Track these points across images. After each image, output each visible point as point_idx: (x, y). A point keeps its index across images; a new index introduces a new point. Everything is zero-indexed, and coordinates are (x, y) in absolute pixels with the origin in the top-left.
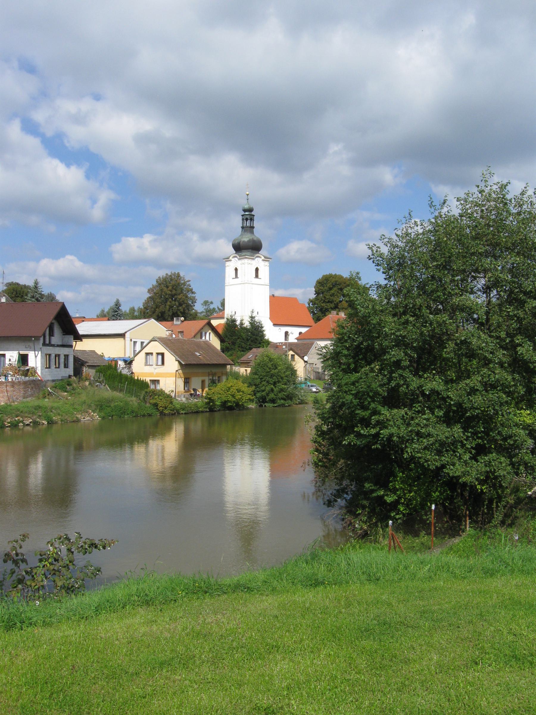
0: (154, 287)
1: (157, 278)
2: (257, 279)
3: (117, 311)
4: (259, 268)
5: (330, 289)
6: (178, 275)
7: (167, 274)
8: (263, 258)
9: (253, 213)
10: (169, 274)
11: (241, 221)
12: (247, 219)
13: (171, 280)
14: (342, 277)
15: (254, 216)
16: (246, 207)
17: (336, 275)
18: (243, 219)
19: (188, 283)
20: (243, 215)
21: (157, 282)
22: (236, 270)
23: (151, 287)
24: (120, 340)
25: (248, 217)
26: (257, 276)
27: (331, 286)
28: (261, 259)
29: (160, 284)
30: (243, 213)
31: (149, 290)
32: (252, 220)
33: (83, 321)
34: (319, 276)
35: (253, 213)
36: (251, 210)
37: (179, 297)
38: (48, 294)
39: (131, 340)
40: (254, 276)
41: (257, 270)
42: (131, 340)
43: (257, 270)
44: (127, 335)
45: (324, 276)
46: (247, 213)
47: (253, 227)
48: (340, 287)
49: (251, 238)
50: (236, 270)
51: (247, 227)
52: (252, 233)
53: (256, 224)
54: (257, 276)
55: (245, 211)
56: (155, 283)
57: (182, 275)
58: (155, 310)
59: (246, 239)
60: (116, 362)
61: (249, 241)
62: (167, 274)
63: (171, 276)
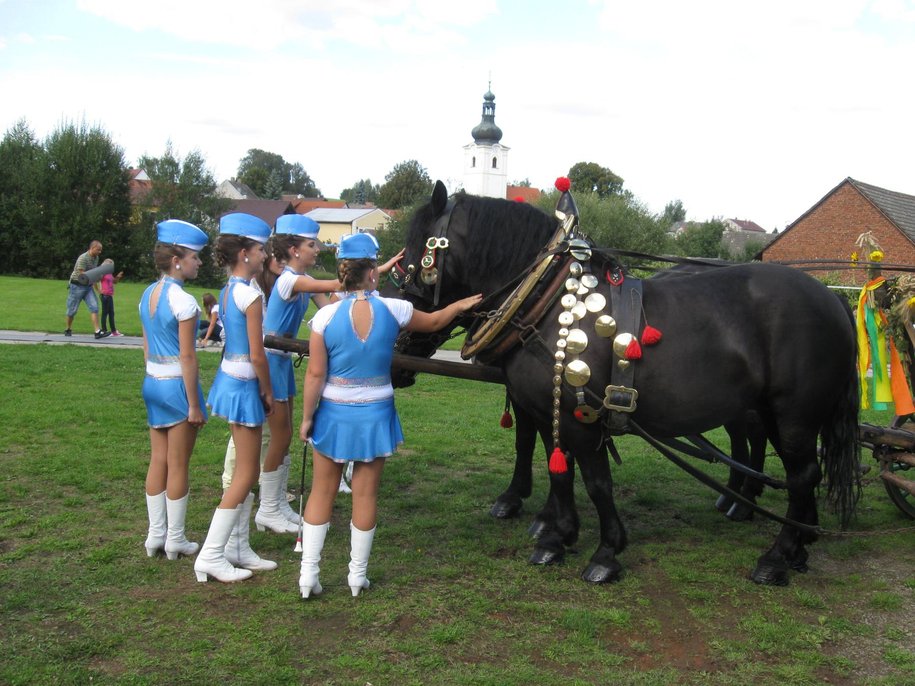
0: (391, 174)
1: (395, 165)
2: (494, 169)
3: (360, 193)
4: (497, 157)
5: (582, 178)
6: (416, 163)
7: (405, 161)
8: (501, 148)
9: (494, 101)
10: (407, 161)
13: (409, 166)
14: (596, 165)
16: (488, 95)
17: (590, 164)
18: (484, 108)
19: (425, 171)
20: (484, 104)
21: (395, 168)
22: (474, 159)
23: (389, 174)
24: (349, 226)
25: (489, 105)
26: (494, 165)
27: (583, 176)
28: (499, 150)
29: (397, 171)
30: (484, 101)
31: (386, 177)
32: (493, 108)
33: (318, 207)
34: (572, 165)
35: (494, 101)
37: (414, 185)
38: (295, 164)
39: (357, 228)
40: (492, 165)
41: (495, 160)
42: (357, 228)
43: (495, 160)
44: (354, 224)
45: (577, 164)
46: (488, 102)
48: (591, 177)
49: (490, 127)
50: (474, 159)
51: (487, 116)
54: (494, 165)
56: (392, 170)
57: (419, 162)
58: (391, 197)
59: (485, 128)
60: (335, 249)
61: (488, 130)
62: (405, 161)
63: (408, 163)
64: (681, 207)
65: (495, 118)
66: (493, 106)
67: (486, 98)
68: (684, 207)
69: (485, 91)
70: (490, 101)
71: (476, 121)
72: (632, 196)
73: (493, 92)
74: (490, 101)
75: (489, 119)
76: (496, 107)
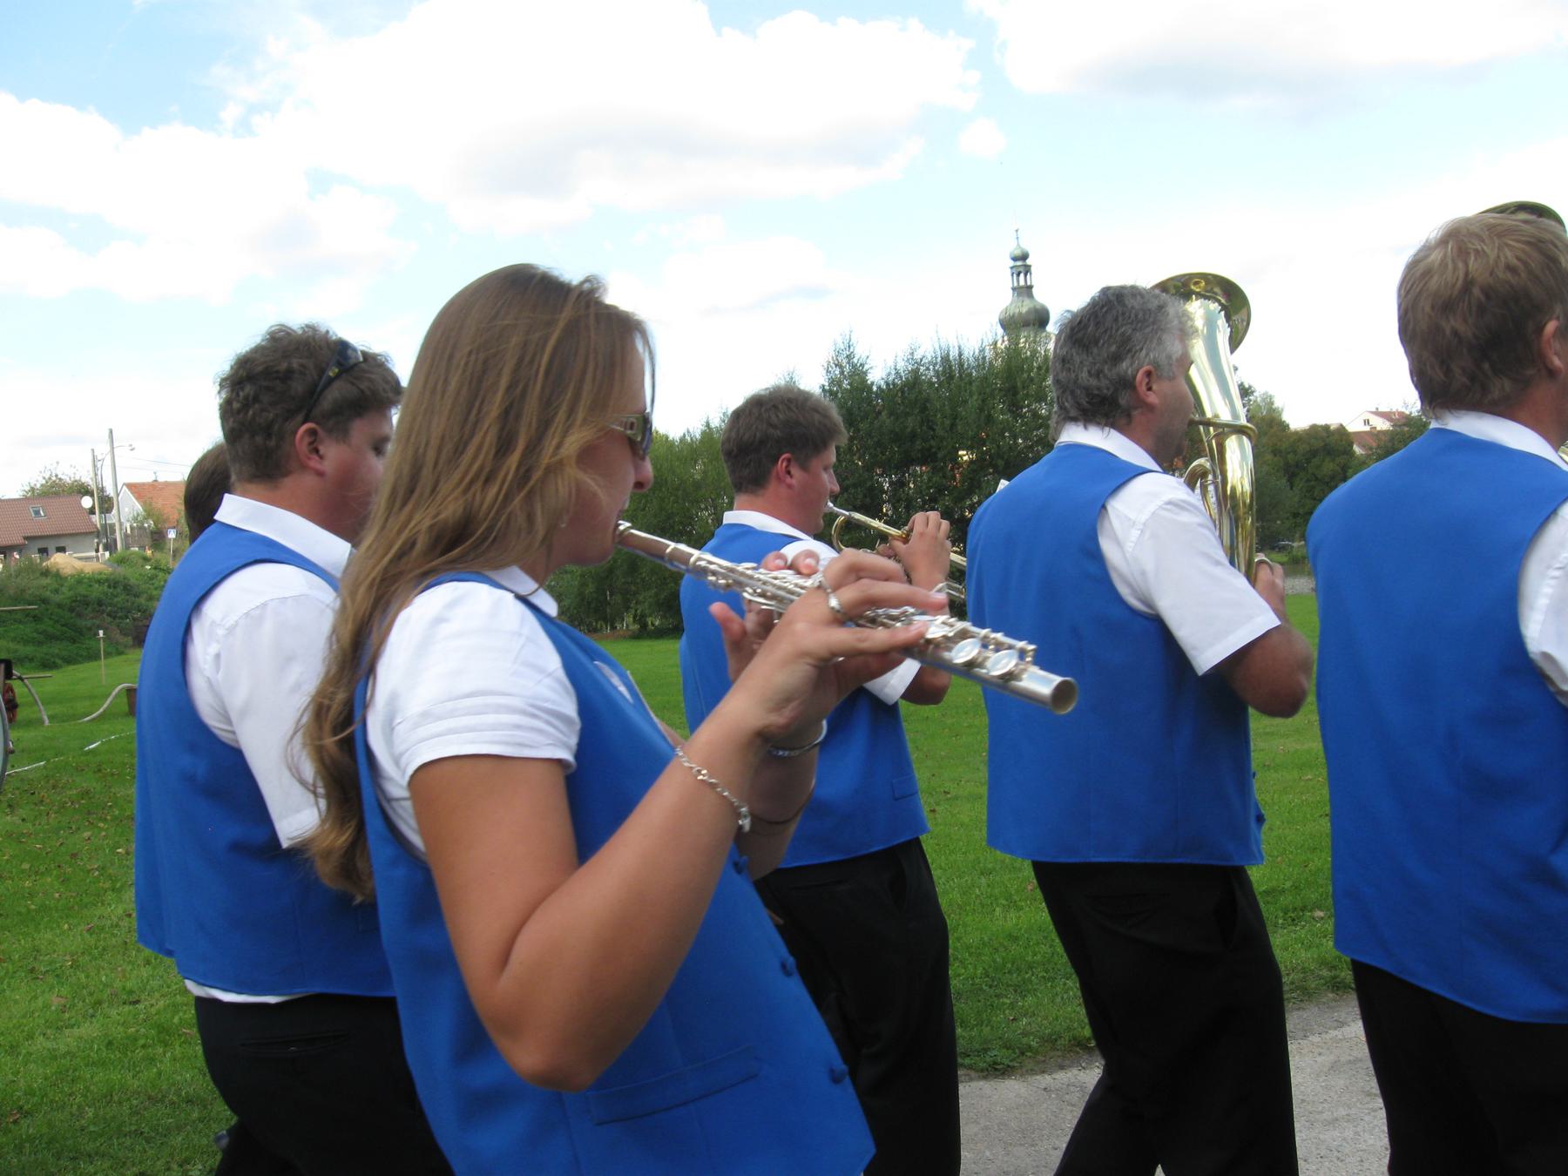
9: (1028, 262)
11: (1011, 277)
12: (1018, 275)
15: (1030, 266)
16: (1018, 253)
20: (1012, 268)
25: (1021, 269)
30: (1012, 263)
35: (1028, 262)
36: (1024, 257)
46: (1019, 263)
47: (1031, 287)
49: (1032, 306)
51: (1022, 287)
52: (1030, 295)
53: (1036, 279)
55: (1015, 259)
59: (1025, 307)
61: (1029, 312)
64: (1272, 404)
65: (1034, 290)
66: (1027, 270)
67: (1015, 259)
68: (1278, 404)
69: (1011, 248)
70: (1021, 264)
71: (1002, 299)
72: (1252, 392)
73: (1027, 246)
74: (1021, 264)
75: (1025, 291)
76: (1032, 269)
